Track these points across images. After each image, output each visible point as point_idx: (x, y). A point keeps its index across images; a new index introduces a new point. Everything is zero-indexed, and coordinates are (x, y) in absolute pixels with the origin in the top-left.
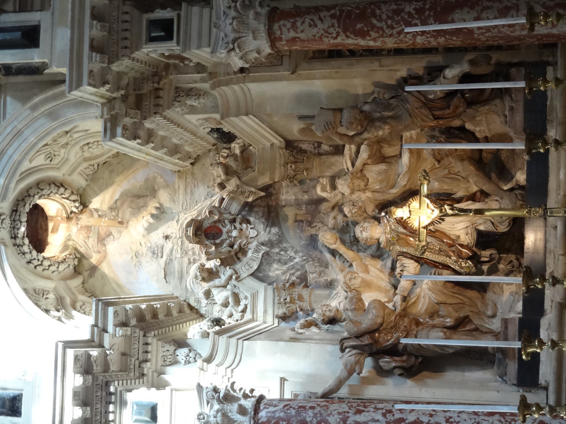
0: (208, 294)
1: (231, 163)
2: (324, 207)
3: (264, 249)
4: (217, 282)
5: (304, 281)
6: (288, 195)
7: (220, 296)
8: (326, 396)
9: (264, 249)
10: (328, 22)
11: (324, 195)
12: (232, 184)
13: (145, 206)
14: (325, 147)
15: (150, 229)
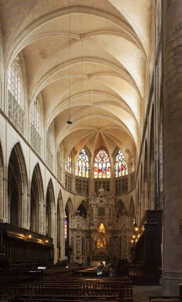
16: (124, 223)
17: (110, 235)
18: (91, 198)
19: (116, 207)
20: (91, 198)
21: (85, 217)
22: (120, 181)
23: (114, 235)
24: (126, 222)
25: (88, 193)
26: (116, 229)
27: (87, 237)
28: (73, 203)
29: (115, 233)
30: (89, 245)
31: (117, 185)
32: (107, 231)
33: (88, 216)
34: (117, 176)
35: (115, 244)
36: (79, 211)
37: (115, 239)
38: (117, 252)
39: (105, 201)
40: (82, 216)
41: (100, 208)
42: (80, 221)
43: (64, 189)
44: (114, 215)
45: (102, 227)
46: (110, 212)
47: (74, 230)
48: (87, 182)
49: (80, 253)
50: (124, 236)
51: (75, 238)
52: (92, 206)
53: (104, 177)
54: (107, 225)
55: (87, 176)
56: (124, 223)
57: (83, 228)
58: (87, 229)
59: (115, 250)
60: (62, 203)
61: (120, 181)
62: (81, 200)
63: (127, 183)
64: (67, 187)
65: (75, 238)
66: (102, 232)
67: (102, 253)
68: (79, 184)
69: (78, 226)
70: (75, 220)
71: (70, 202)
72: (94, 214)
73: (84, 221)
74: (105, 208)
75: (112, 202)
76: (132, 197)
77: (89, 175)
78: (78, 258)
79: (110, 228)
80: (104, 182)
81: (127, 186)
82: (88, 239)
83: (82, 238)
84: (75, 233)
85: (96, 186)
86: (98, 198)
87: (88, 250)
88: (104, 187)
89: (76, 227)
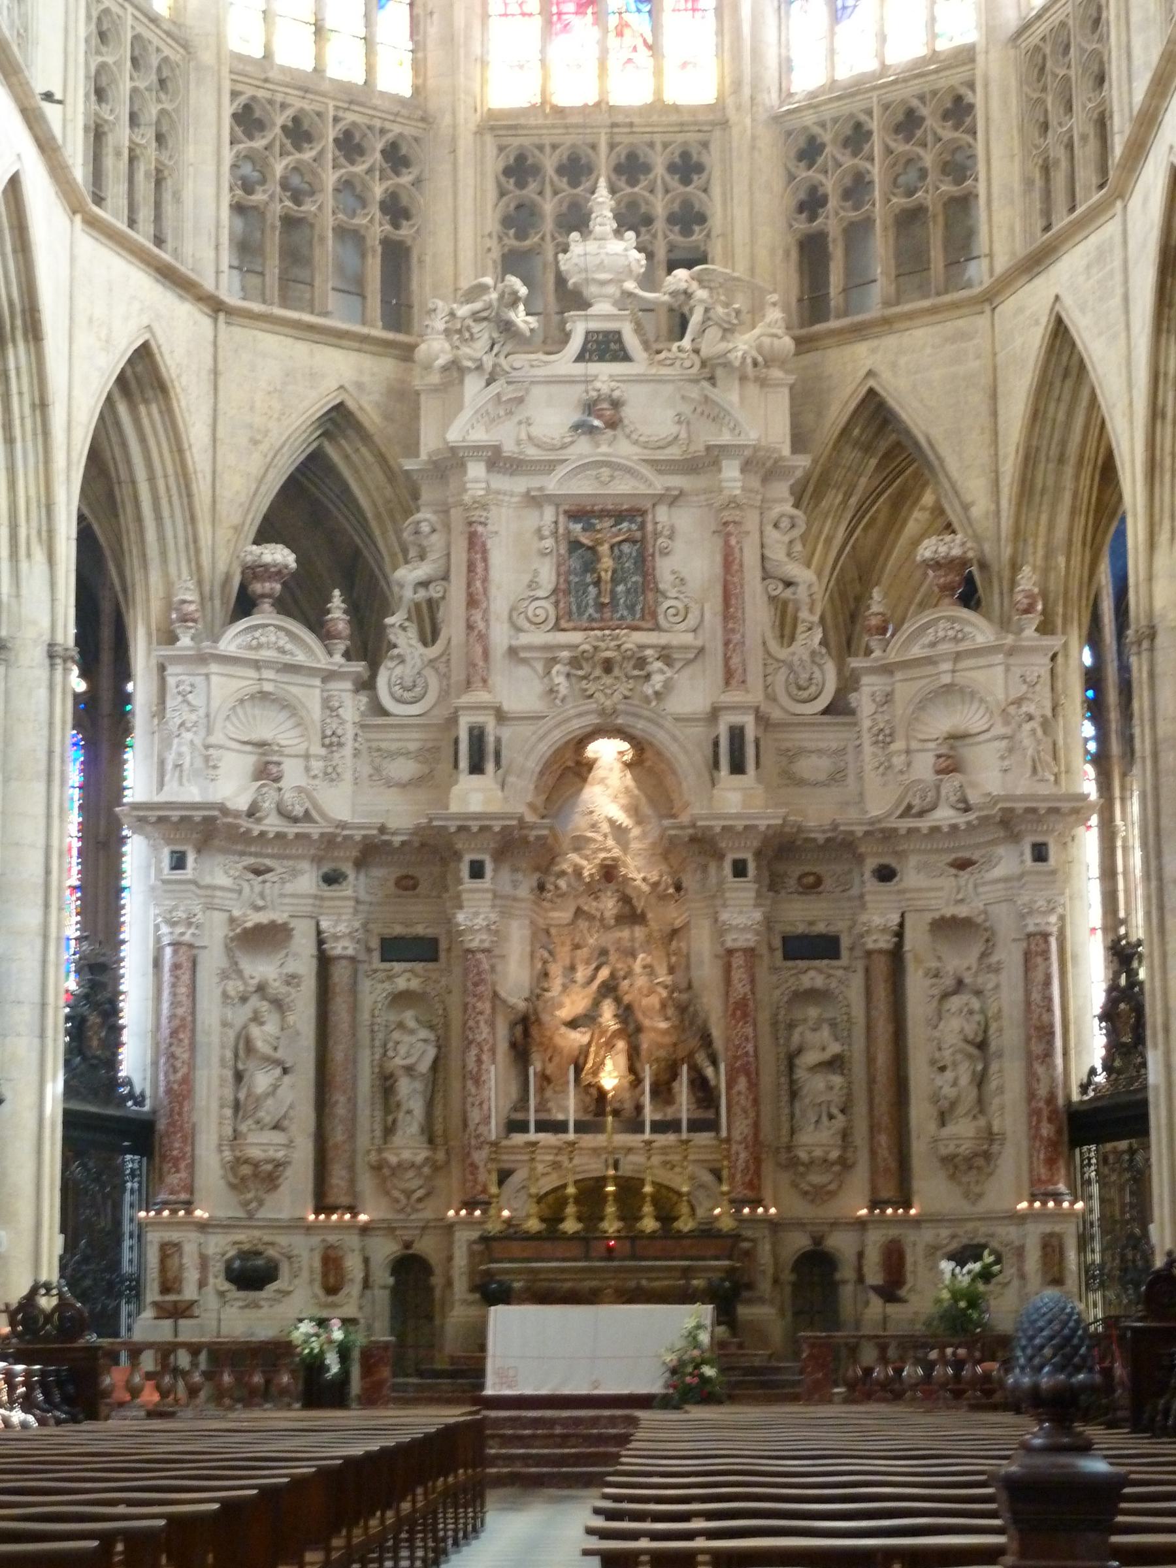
0: (563, 873)
1: (662, 887)
2: (630, 960)
3: (598, 915)
4: (573, 880)
5: (577, 947)
6: (639, 932)
7: (562, 883)
8: (496, 995)
9: (598, 915)
10: (742, 991)
11: (639, 960)
12: (645, 888)
13: (630, 816)
14: (674, 959)
15: (611, 822)
16: (942, 722)
17: (742, 913)
18: (455, 370)
19: (808, 493)
20: (455, 370)
21: (369, 646)
22: (856, 138)
23: (804, 914)
24: (969, 718)
25: (399, 311)
26: (817, 813)
27: (395, 949)
28: (196, 433)
29: (812, 886)
30: (424, 1067)
31: (811, 203)
32: (694, 849)
33: (399, 628)
34: (807, 79)
35: (819, 1044)
36: (280, 555)
37: (813, 975)
38: (845, 1165)
39: (655, 411)
40: (317, 625)
41: (581, 513)
42: (286, 705)
43: (75, 208)
44: (786, 625)
45: (608, 791)
46: (729, 562)
47: (198, 832)
48: (396, 158)
49: (292, 1199)
50: (948, 927)
51: (212, 960)
52: (476, 470)
53: (630, 90)
54: (685, 752)
55: (395, 80)
56: (942, 722)
57: (345, 804)
58: (399, 814)
59: (817, 1139)
60: (42, 405)
61: (856, 138)
62: (313, 403)
63: (958, 167)
64: (115, 167)
65: (212, 960)
66: (609, 872)
67: (629, 1189)
68: (279, 167)
69: (266, 772)
70: (224, 686)
71: (151, 414)
72: (499, 602)
73: (351, 706)
74: (662, 514)
75: (764, 421)
76: (1060, 332)
77: (418, 67)
78: (251, 1275)
79: (736, 800)
80: (631, 168)
81: (961, 205)
82: (406, 976)
83: (324, 962)
84: (219, 872)
85: (520, 219)
86: (564, 362)
87: (408, 1146)
88: (631, 218)
89: (231, 787)
